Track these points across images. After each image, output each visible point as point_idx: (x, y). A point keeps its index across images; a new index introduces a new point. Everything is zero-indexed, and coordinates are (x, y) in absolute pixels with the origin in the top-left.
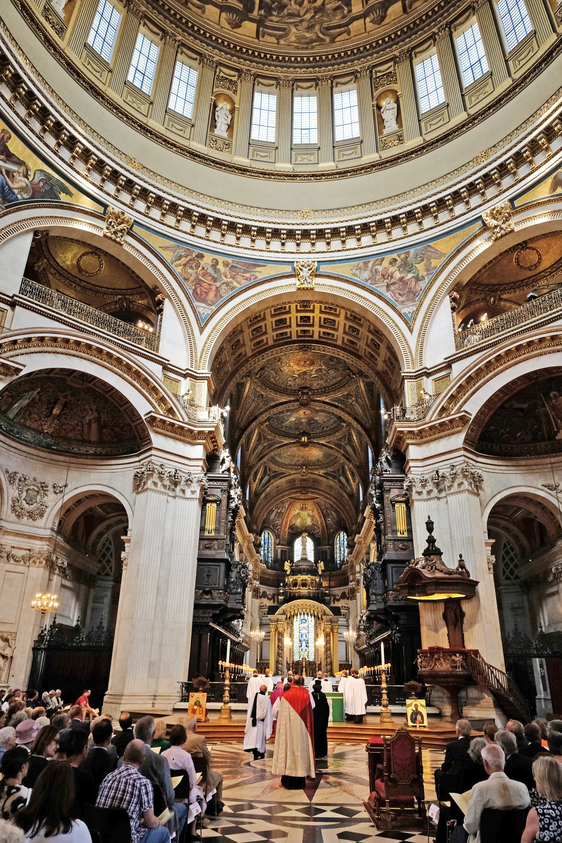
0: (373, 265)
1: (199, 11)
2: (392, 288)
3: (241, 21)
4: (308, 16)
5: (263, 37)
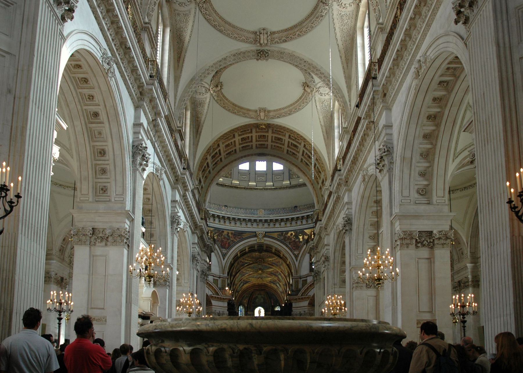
0: (285, 234)
2: (291, 244)
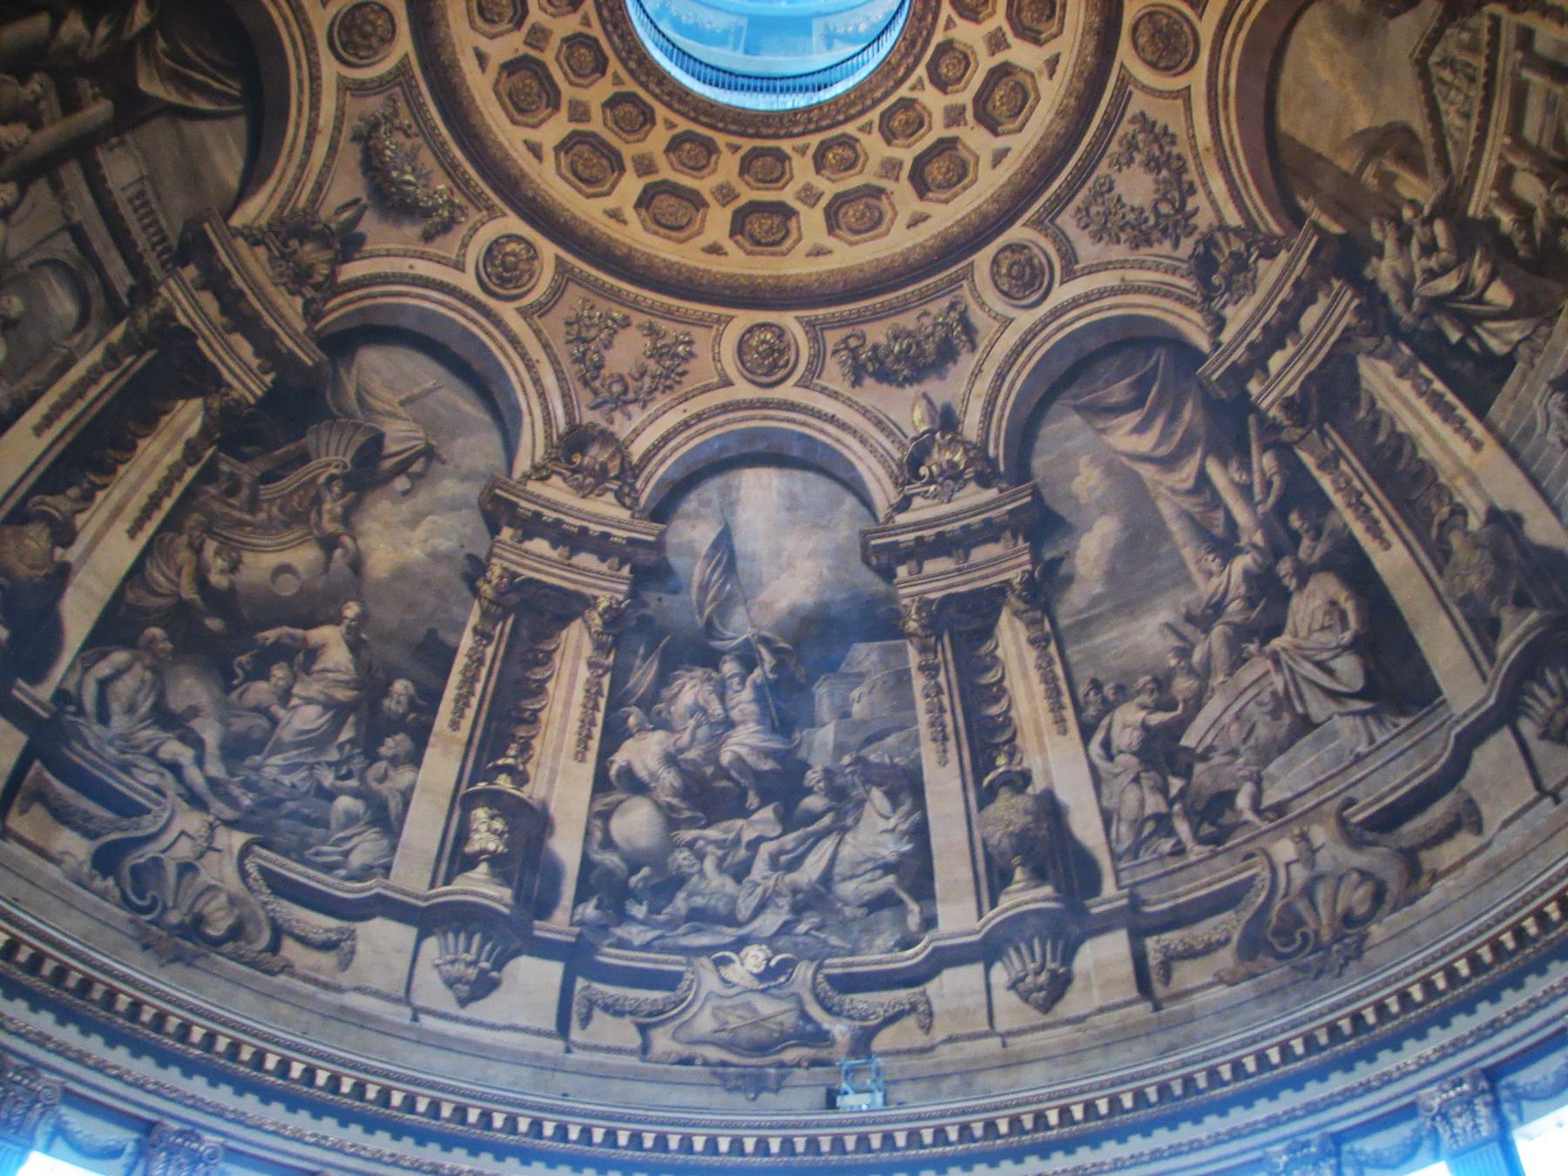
1: (327, 960)
3: (499, 965)
4: (770, 922)
5: (586, 1020)
